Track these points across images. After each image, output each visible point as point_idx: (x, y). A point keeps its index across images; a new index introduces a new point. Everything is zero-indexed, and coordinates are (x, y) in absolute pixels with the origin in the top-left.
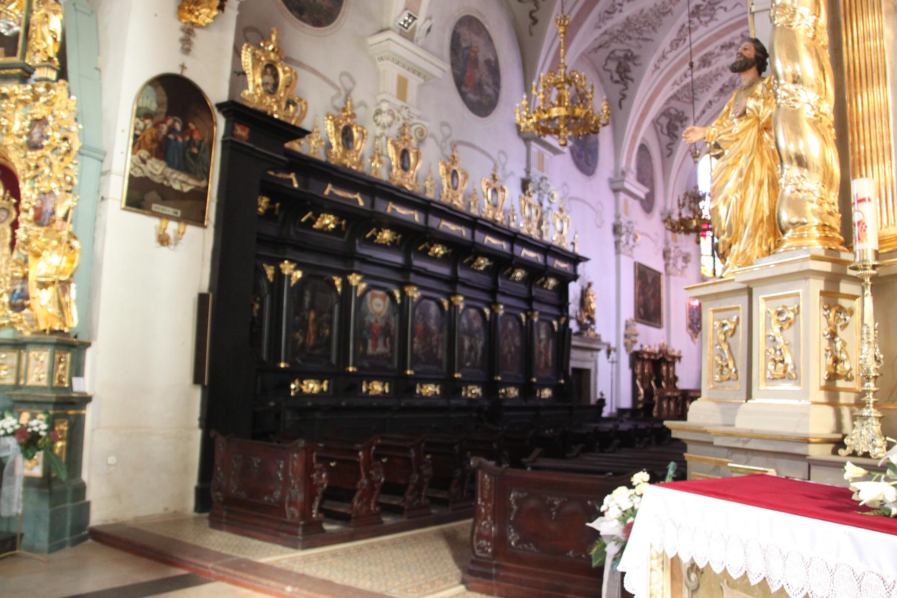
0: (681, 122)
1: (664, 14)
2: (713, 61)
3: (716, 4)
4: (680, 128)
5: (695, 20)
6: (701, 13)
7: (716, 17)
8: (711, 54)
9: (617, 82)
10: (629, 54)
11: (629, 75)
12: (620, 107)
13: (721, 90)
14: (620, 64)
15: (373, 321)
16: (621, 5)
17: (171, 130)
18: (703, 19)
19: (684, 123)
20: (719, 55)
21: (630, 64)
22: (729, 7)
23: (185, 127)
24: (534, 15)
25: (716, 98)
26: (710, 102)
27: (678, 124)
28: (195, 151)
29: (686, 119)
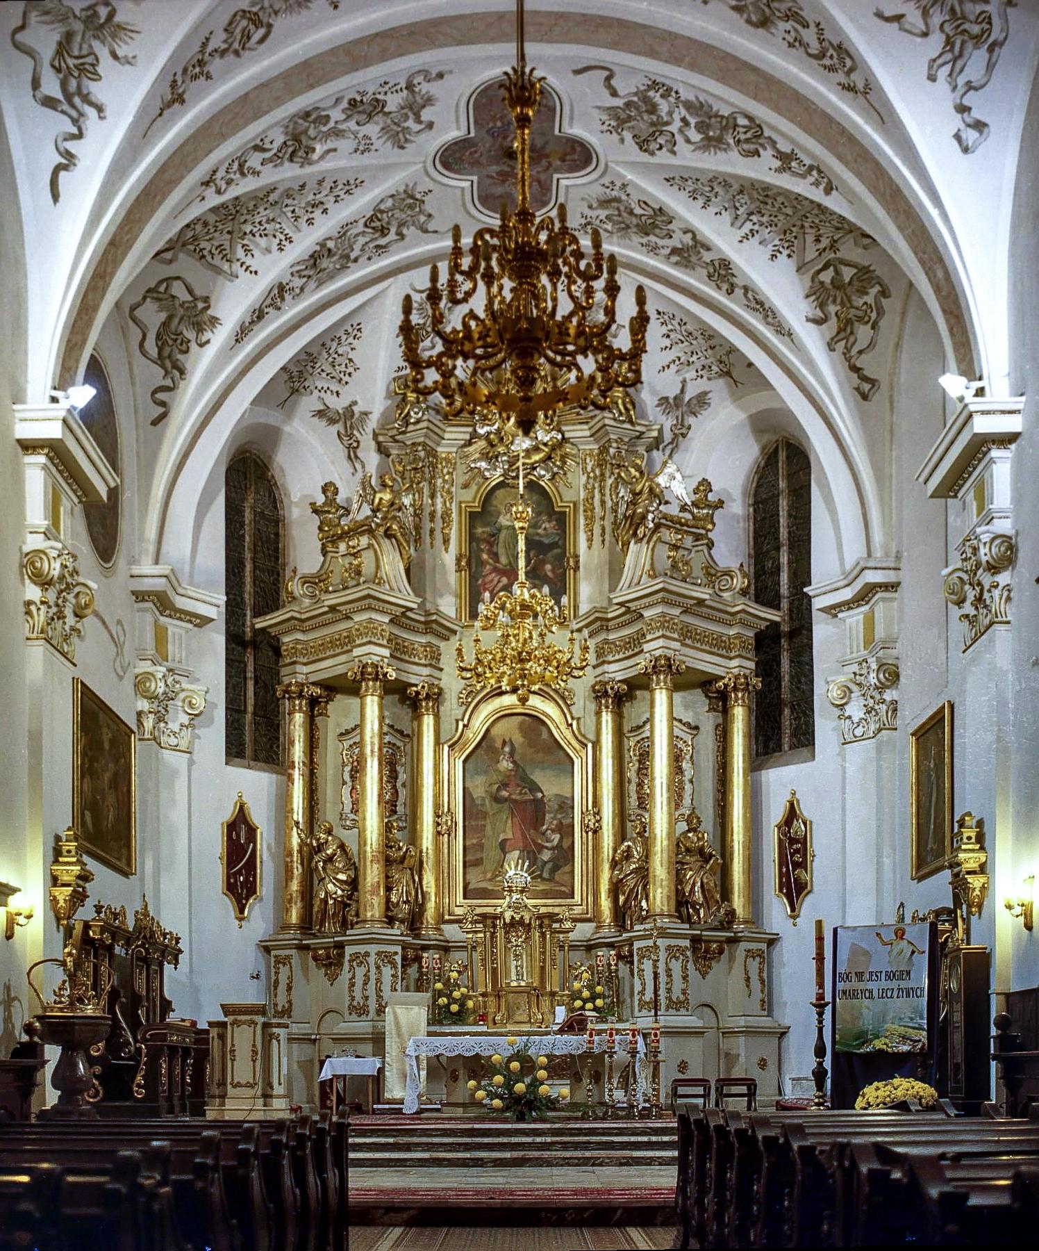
2: (319, 148)
13: (314, 258)
14: (69, 36)
20: (337, 133)
21: (96, 45)
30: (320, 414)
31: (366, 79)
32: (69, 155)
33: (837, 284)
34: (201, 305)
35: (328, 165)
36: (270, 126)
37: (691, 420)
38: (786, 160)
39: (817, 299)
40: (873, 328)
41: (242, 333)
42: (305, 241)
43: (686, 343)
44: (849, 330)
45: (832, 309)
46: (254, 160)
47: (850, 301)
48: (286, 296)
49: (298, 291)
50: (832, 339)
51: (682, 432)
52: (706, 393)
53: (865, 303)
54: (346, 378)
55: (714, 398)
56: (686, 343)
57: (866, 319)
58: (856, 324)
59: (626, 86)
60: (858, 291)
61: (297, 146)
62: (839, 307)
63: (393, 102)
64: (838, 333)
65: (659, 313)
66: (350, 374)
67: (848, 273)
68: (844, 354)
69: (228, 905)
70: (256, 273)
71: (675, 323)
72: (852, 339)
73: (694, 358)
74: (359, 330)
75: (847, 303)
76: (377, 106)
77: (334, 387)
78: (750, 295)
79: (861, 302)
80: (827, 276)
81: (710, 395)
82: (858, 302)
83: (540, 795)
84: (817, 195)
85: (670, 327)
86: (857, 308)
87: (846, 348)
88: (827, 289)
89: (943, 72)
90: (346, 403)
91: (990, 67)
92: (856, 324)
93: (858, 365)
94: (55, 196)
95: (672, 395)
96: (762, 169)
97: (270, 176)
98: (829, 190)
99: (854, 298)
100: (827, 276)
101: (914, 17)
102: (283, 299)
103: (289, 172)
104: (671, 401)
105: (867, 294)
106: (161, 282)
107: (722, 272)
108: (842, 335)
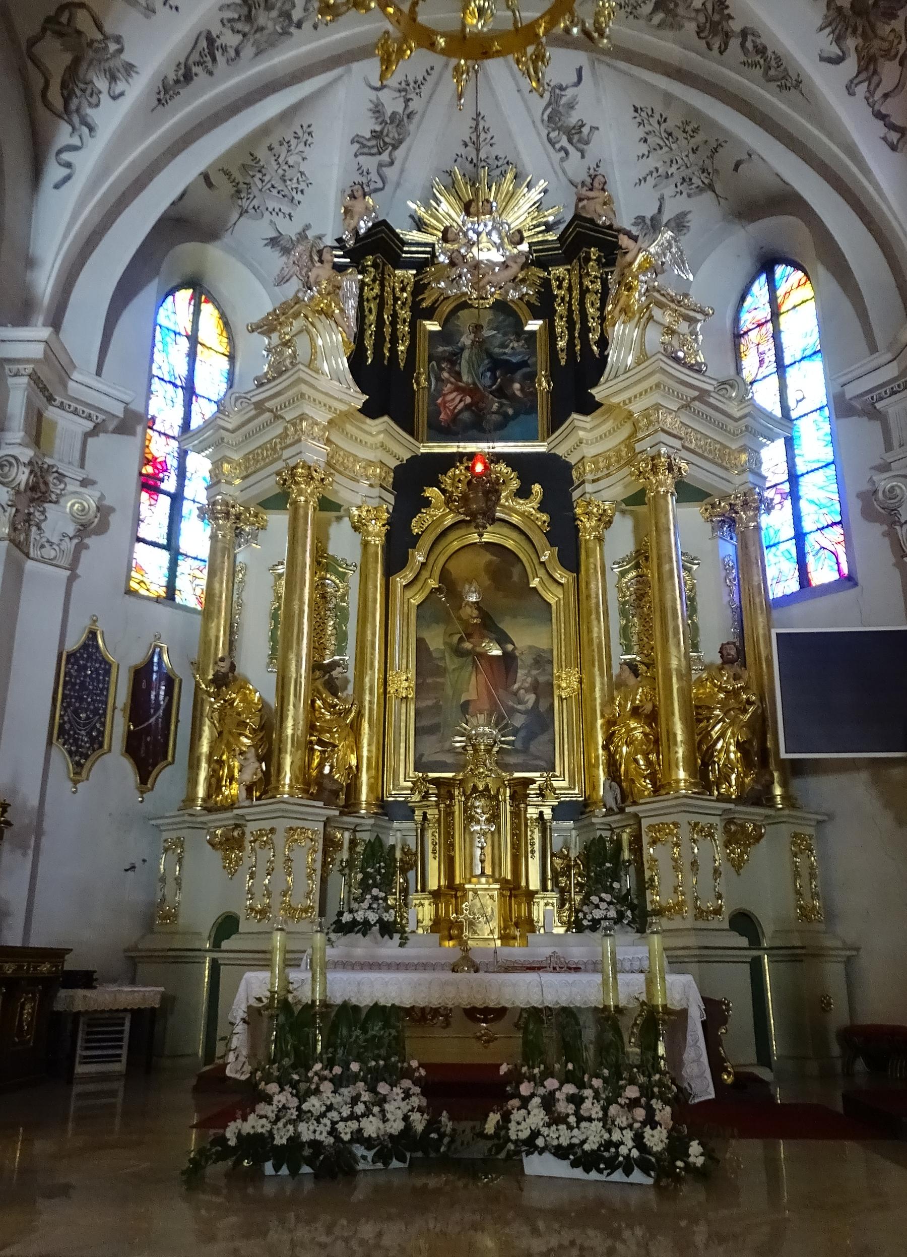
0: (113, 78)
4: (104, 97)
19: (120, 87)
25: (230, 39)
29: (129, 68)
30: (273, 242)
34: (113, 47)
39: (833, 32)
40: (901, 63)
43: (665, 149)
44: (872, 67)
45: (851, 43)
47: (874, 31)
48: (218, 54)
49: (232, 53)
50: (851, 81)
52: (684, 214)
53: (893, 30)
54: (298, 197)
55: (694, 221)
56: (665, 149)
57: (893, 52)
58: (881, 60)
60: (884, 14)
62: (860, 40)
64: (859, 73)
65: (636, 110)
66: (302, 192)
68: (867, 99)
70: (177, 8)
71: (654, 121)
72: (875, 80)
73: (673, 169)
74: (310, 134)
77: (286, 210)
78: (749, 45)
79: (888, 29)
81: (689, 217)
82: (884, 29)
83: (510, 647)
85: (648, 128)
86: (882, 39)
87: (868, 91)
88: (845, 17)
90: (299, 229)
92: (881, 60)
93: (884, 112)
95: (648, 215)
99: (879, 25)
102: (214, 60)
104: (648, 222)
105: (894, 16)
106: (62, 8)
108: (863, 76)
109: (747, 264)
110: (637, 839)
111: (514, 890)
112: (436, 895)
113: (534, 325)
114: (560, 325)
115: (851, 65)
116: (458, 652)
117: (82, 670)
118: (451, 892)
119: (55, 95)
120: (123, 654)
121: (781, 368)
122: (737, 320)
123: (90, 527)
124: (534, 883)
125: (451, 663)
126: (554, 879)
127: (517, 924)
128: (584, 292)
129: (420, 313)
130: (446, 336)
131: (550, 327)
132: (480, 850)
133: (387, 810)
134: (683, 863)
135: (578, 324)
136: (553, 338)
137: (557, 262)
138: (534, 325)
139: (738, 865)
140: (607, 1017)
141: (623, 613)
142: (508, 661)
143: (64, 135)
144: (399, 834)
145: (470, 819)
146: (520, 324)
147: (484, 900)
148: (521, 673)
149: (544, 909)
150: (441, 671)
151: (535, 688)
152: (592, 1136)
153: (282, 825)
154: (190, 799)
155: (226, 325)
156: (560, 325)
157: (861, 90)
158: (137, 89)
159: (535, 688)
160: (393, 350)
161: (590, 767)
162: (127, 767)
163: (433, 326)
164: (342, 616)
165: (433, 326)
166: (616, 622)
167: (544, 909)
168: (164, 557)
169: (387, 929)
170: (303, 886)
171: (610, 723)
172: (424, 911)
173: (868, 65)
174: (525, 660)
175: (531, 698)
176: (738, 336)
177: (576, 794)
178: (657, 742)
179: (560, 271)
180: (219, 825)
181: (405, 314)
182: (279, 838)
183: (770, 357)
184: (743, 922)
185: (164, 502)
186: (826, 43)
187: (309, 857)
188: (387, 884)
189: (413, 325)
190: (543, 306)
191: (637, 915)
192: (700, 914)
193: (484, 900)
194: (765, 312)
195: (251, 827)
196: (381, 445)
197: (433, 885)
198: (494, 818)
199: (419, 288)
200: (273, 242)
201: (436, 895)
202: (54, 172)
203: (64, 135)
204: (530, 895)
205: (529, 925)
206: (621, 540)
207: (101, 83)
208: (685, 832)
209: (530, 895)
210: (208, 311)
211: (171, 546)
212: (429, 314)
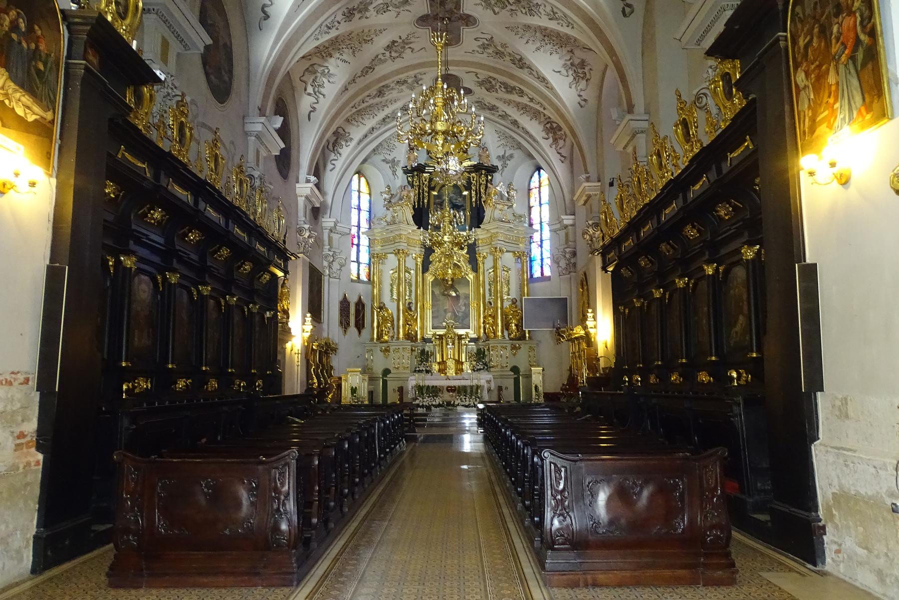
1: (366, 41)
3: (407, 44)
5: (388, 54)
6: (394, 48)
7: (403, 55)
8: (387, 86)
9: (309, 94)
10: (326, 71)
11: (322, 90)
12: (309, 119)
15: (139, 309)
16: (339, 23)
17: (14, 27)
18: (394, 54)
20: (392, 89)
21: (324, 79)
22: (416, 49)
23: (30, 29)
24: (266, 9)
26: (373, 129)
27: (343, 143)
28: (41, 67)
29: (351, 139)
31: (402, 77)
32: (314, 108)
33: (552, 128)
35: (390, 97)
36: (373, 91)
37: (508, 162)
38: (532, 100)
41: (360, 141)
42: (381, 115)
45: (551, 135)
46: (367, 99)
51: (505, 166)
55: (516, 156)
59: (482, 77)
61: (380, 93)
63: (410, 81)
67: (555, 125)
69: (341, 331)
75: (555, 133)
76: (405, 82)
80: (548, 126)
84: (541, 109)
89: (573, 86)
91: (587, 85)
94: (309, 119)
96: (525, 100)
97: (372, 101)
98: (544, 109)
100: (548, 126)
101: (564, 72)
103: (378, 100)
107: (515, 123)
109: (533, 168)
110: (488, 350)
111: (459, 362)
112: (439, 363)
113: (465, 193)
114: (473, 193)
115: (551, 140)
116: (444, 295)
117: (344, 304)
118: (443, 363)
119: (331, 147)
120: (353, 300)
121: (541, 205)
122: (529, 184)
123: (342, 266)
124: (464, 360)
125: (441, 298)
126: (470, 356)
127: (459, 370)
128: (480, 185)
129: (431, 188)
130: (439, 196)
131: (471, 193)
132: (450, 350)
133: (425, 340)
134: (500, 356)
135: (478, 193)
136: (471, 198)
137: (472, 172)
138: (465, 193)
139: (514, 355)
140: (472, 387)
141: (490, 285)
142: (458, 297)
143: (333, 156)
144: (428, 347)
145: (447, 344)
146: (461, 192)
147: (451, 364)
148: (461, 301)
149: (466, 367)
150: (438, 300)
151: (465, 305)
152: (467, 403)
153: (401, 347)
154: (372, 339)
155: (368, 183)
156: (473, 193)
157: (554, 146)
158: (353, 144)
159: (465, 305)
160: (423, 202)
161: (480, 328)
162: (355, 330)
163: (435, 193)
164: (410, 285)
165: (435, 193)
166: (487, 287)
167: (466, 367)
168: (356, 264)
169: (427, 372)
170: (406, 362)
171: (484, 317)
172: (436, 367)
173: (555, 140)
174: (462, 296)
175: (464, 308)
176: (530, 190)
177: (475, 336)
178: (495, 323)
179: (474, 174)
180: (384, 346)
181: (426, 189)
182: (401, 350)
183: (538, 199)
184: (515, 369)
185: (355, 247)
186: (544, 134)
187: (407, 354)
188: (427, 361)
189: (429, 193)
190: (468, 187)
191: (487, 367)
192: (502, 367)
193: (451, 364)
194: (537, 185)
195: (392, 349)
196: (419, 235)
197: (438, 361)
198: (453, 344)
199: (431, 180)
200: (384, 161)
201: (439, 363)
202: (329, 166)
203: (333, 156)
204: (462, 363)
205: (462, 370)
206: (489, 262)
207: (343, 143)
208: (499, 348)
209: (462, 363)
210: (363, 179)
211: (358, 262)
212: (433, 189)
